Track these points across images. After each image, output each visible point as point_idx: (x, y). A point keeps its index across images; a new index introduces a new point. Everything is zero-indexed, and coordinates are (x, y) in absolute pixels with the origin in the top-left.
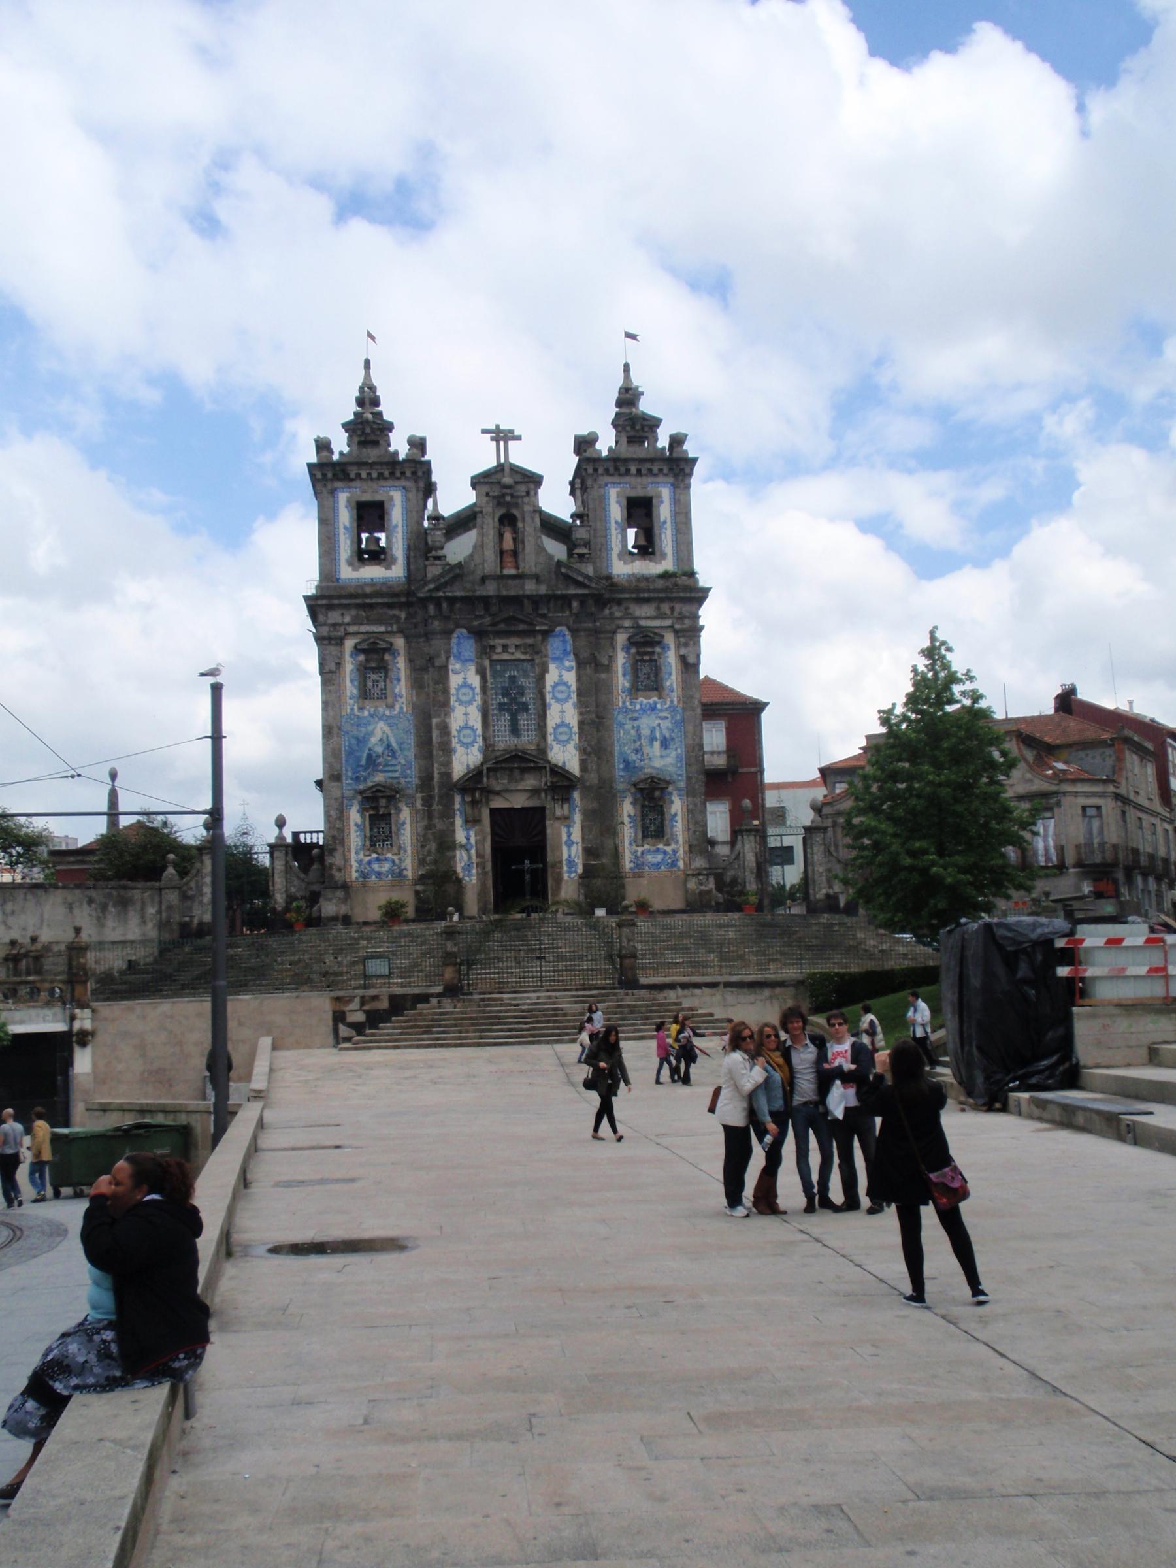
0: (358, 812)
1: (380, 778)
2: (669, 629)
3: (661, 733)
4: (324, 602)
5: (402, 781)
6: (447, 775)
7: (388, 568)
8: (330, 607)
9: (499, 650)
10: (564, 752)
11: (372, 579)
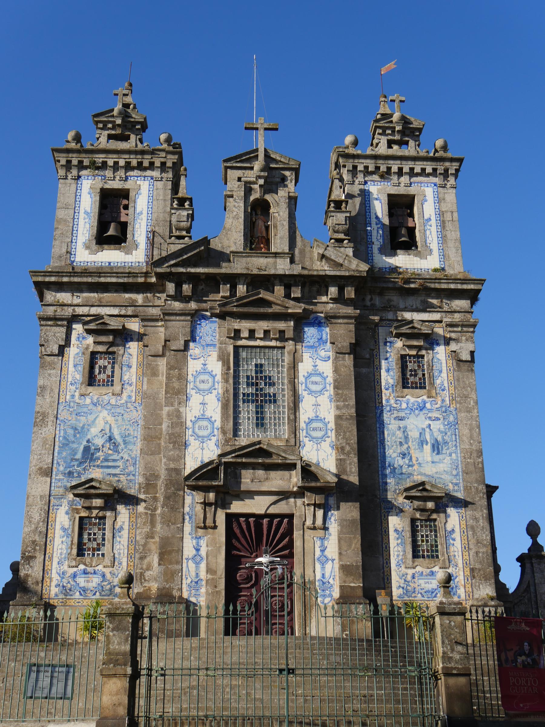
0: (67, 513)
1: (96, 474)
2: (437, 324)
3: (432, 435)
4: (53, 279)
5: (123, 478)
6: (178, 471)
7: (128, 252)
8: (60, 287)
9: (245, 334)
10: (318, 450)
11: (110, 263)
